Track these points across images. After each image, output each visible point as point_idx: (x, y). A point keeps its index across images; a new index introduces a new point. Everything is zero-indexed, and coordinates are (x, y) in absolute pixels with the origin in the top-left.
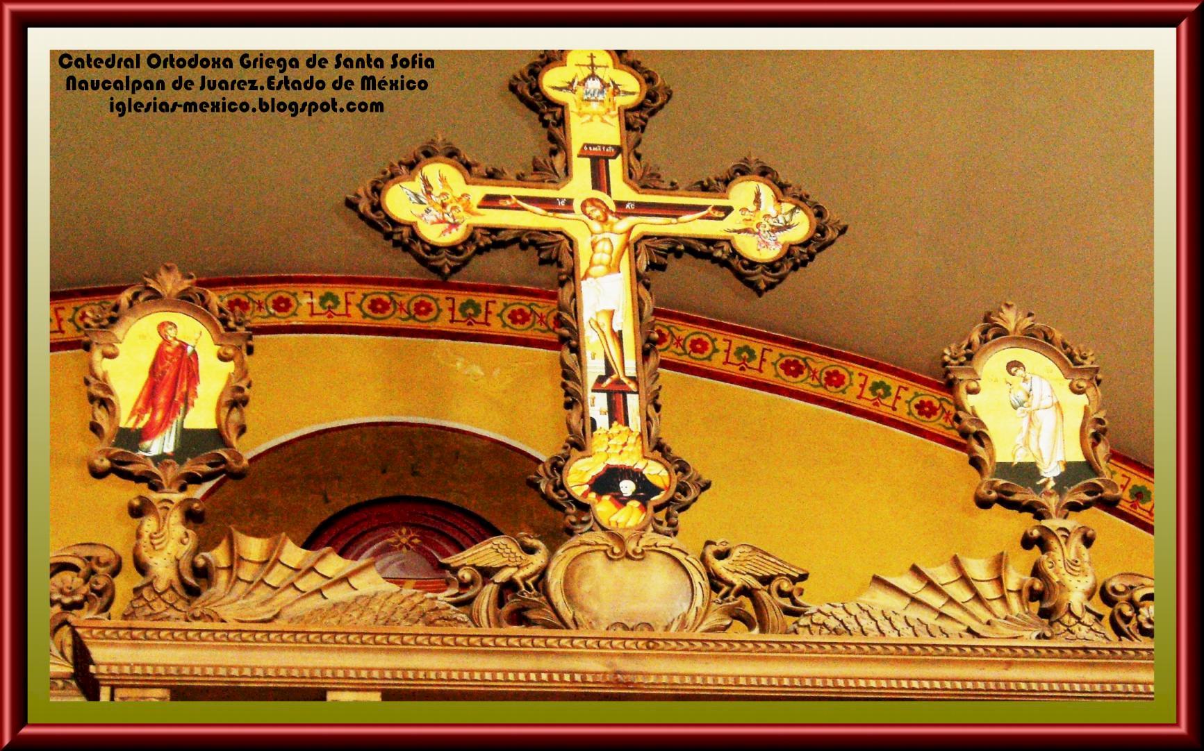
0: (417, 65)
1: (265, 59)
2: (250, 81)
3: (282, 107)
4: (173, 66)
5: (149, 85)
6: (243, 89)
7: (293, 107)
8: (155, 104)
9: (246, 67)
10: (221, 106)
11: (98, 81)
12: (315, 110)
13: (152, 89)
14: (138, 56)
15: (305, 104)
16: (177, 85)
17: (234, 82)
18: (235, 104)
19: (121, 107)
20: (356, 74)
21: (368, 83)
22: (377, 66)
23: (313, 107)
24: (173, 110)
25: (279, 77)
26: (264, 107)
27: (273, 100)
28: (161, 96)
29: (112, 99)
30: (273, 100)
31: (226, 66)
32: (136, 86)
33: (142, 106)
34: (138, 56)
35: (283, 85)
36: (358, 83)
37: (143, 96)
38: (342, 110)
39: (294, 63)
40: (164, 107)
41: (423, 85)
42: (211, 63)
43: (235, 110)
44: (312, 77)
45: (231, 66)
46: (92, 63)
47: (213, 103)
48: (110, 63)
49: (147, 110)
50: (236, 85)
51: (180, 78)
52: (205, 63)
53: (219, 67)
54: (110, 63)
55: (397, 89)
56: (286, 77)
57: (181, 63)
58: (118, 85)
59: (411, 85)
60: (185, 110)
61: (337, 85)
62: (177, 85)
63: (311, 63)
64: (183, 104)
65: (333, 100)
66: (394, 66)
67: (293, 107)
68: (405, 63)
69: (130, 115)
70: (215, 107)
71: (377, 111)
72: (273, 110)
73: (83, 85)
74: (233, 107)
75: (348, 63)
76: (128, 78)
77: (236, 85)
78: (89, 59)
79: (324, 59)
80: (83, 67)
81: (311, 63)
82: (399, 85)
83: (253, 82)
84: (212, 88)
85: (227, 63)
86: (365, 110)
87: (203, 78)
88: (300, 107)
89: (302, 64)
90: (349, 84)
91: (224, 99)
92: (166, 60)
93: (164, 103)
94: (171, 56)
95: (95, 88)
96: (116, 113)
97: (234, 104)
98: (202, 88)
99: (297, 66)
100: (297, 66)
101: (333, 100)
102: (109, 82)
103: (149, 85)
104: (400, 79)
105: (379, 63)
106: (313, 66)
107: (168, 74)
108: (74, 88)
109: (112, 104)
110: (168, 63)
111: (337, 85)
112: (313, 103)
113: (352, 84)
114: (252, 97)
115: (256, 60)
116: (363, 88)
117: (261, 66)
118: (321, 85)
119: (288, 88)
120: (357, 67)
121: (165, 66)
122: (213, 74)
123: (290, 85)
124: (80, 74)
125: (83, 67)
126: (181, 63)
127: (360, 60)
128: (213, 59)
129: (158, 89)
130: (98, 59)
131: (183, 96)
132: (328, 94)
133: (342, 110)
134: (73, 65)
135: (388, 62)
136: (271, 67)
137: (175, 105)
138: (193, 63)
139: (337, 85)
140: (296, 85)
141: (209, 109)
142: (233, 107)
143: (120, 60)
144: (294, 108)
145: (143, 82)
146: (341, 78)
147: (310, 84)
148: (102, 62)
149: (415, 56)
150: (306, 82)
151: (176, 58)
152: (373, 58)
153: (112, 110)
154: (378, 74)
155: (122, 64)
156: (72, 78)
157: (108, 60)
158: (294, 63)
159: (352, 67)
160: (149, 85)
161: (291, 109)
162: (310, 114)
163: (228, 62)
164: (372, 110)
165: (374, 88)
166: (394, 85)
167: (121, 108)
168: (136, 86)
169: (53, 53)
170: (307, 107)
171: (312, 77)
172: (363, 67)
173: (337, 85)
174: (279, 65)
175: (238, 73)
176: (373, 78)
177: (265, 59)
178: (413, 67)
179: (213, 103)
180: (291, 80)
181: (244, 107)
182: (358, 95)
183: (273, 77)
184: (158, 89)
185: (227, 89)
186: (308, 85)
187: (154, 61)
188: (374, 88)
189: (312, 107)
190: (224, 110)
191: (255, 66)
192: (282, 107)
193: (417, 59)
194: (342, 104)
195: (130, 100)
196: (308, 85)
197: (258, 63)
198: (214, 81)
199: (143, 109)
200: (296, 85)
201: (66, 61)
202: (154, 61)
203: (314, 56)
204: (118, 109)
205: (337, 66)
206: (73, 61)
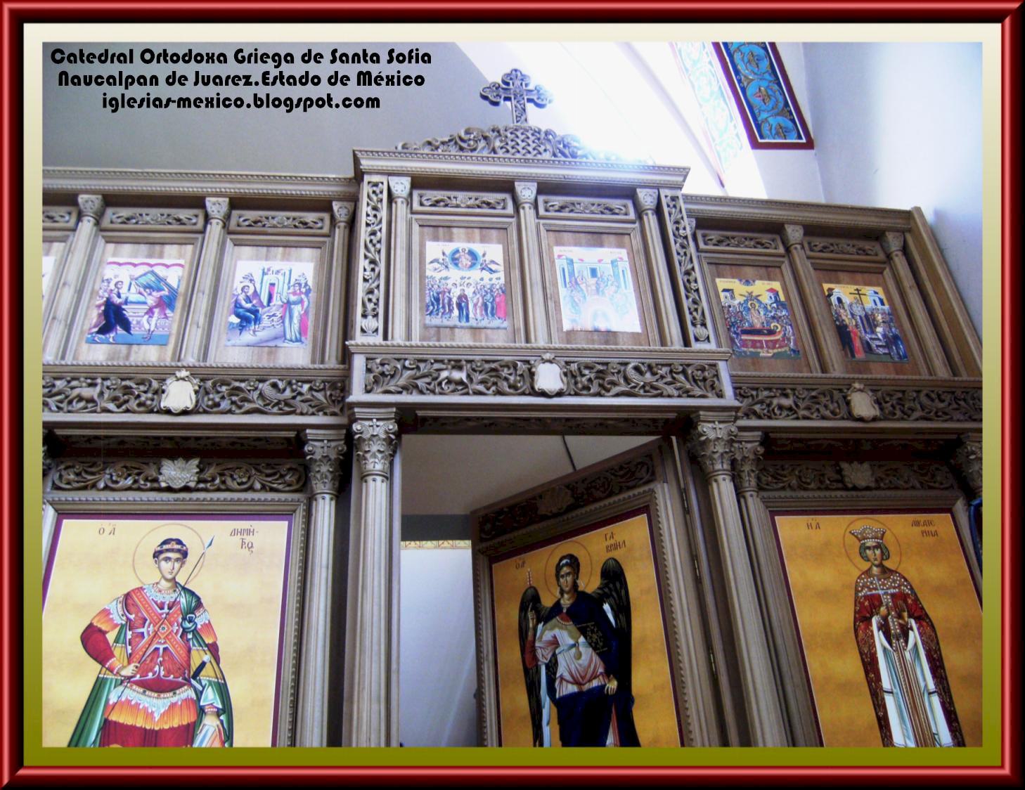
0: (413, 61)
2: (244, 77)
3: (277, 103)
4: (166, 61)
5: (142, 80)
6: (238, 84)
7: (288, 102)
8: (148, 99)
9: (241, 62)
10: (215, 102)
11: (91, 77)
12: (310, 106)
13: (145, 84)
14: (131, 51)
15: (300, 100)
16: (171, 80)
17: (228, 77)
18: (229, 100)
19: (114, 102)
20: (351, 70)
21: (364, 78)
22: (373, 61)
23: (308, 103)
24: (167, 106)
25: (274, 72)
26: (258, 103)
27: (268, 95)
28: (154, 92)
29: (105, 94)
30: (268, 95)
31: (220, 62)
32: (130, 81)
33: (135, 102)
34: (131, 51)
35: (278, 81)
36: (354, 79)
37: (137, 92)
38: (337, 106)
39: (289, 58)
40: (157, 103)
41: (420, 80)
42: (205, 58)
43: (229, 106)
44: (307, 73)
45: (225, 61)
46: (85, 58)
47: (207, 99)
48: (103, 58)
49: (140, 106)
50: (230, 81)
51: (174, 73)
52: (199, 58)
53: (213, 62)
54: (103, 58)
55: (393, 84)
56: (281, 73)
57: (175, 58)
58: (111, 81)
60: (179, 106)
61: (333, 80)
62: (171, 80)
63: (306, 58)
64: (176, 99)
65: (329, 95)
66: (390, 61)
67: (288, 102)
68: (401, 58)
69: (124, 111)
70: (209, 103)
71: (373, 106)
72: (268, 106)
73: (76, 81)
74: (227, 103)
75: (344, 58)
76: (121, 73)
77: (230, 81)
78: (82, 55)
79: (319, 54)
80: (75, 62)
82: (395, 80)
83: (247, 77)
84: (206, 84)
85: (222, 58)
86: (360, 106)
87: (197, 73)
88: (295, 102)
89: (298, 58)
90: (345, 80)
91: (218, 94)
92: (159, 55)
93: (157, 99)
94: (165, 51)
95: (88, 84)
96: (109, 108)
97: (229, 99)
98: (196, 84)
99: (292, 62)
100: (292, 61)
101: (329, 95)
103: (142, 81)
104: (396, 75)
105: (375, 58)
106: (308, 62)
108: (67, 84)
109: (105, 99)
110: (162, 58)
111: (333, 81)
112: (308, 99)
113: (348, 79)
114: (247, 93)
115: (250, 55)
116: (359, 84)
117: (256, 62)
118: (316, 81)
119: (283, 84)
120: (353, 62)
121: (158, 61)
122: (207, 69)
123: (285, 81)
125: (75, 62)
126: (175, 58)
127: (356, 55)
128: (208, 54)
129: (151, 84)
130: (91, 54)
131: (177, 92)
132: (322, 90)
133: (337, 106)
134: (66, 59)
135: (384, 57)
136: (266, 62)
137: (169, 100)
138: (187, 58)
139: (333, 81)
140: (291, 81)
141: (203, 105)
142: (227, 103)
143: (113, 55)
144: (289, 104)
146: (336, 73)
147: (305, 80)
148: (94, 57)
149: (411, 51)
150: (302, 77)
151: (170, 53)
152: (369, 53)
153: (105, 106)
154: (374, 69)
155: (115, 59)
156: (64, 73)
157: (101, 55)
158: (289, 58)
159: (348, 62)
160: (142, 81)
161: (287, 106)
162: (305, 110)
163: (222, 58)
164: (368, 106)
165: (370, 84)
166: (390, 80)
167: (114, 104)
168: (130, 81)
169: (45, 45)
170: (302, 104)
171: (307, 73)
172: (359, 62)
173: (333, 80)
174: (274, 61)
175: (232, 68)
176: (369, 73)
178: (410, 62)
179: (207, 99)
180: (286, 75)
181: (239, 103)
182: (354, 90)
183: (267, 73)
184: (151, 84)
185: (221, 84)
186: (304, 81)
187: (148, 56)
188: (370, 84)
189: (308, 103)
190: (218, 106)
191: (249, 62)
192: (277, 103)
193: (414, 54)
195: (123, 95)
196: (304, 81)
197: (253, 59)
198: (209, 77)
199: (136, 105)
200: (291, 81)
201: (58, 56)
202: (148, 56)
203: (310, 51)
204: (111, 105)
205: (333, 61)
206: (66, 56)
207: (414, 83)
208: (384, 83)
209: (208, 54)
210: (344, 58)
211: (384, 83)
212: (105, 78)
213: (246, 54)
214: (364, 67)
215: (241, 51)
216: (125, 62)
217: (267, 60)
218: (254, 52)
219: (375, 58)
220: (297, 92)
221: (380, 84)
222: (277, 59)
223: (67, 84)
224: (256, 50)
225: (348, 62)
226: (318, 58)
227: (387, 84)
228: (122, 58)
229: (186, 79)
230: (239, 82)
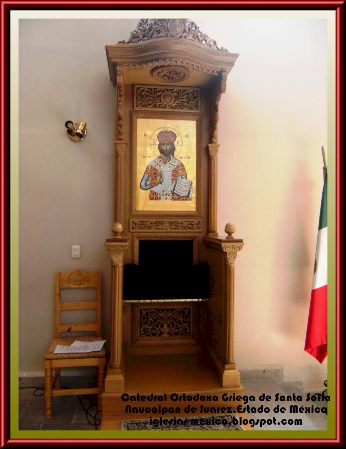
0: (321, 400)
1: (236, 396)
2: (228, 408)
4: (185, 400)
7: (252, 422)
9: (226, 400)
12: (264, 424)
15: (258, 420)
17: (219, 409)
20: (287, 405)
21: (293, 409)
22: (298, 400)
23: (263, 422)
24: (185, 424)
25: (244, 406)
27: (241, 418)
32: (164, 411)
35: (246, 410)
36: (288, 409)
39: (252, 398)
42: (206, 398)
44: (262, 406)
51: (189, 406)
53: (210, 400)
54: (150, 398)
56: (248, 406)
59: (318, 410)
60: (192, 424)
61: (276, 410)
63: (262, 398)
65: (274, 418)
66: (308, 400)
67: (252, 422)
71: (298, 424)
76: (160, 406)
77: (220, 410)
81: (262, 398)
82: (311, 410)
84: (206, 412)
86: (291, 424)
88: (256, 422)
89: (257, 399)
92: (181, 397)
101: (274, 418)
102: (150, 409)
104: (311, 407)
107: (183, 404)
110: (182, 399)
112: (262, 420)
113: (285, 409)
115: (231, 397)
116: (291, 412)
117: (234, 400)
119: (249, 412)
120: (288, 400)
121: (180, 400)
122: (207, 404)
123: (250, 410)
124: (133, 405)
125: (135, 400)
127: (289, 397)
128: (207, 396)
129: (176, 412)
133: (279, 424)
134: (129, 399)
135: (305, 398)
136: (239, 401)
140: (253, 410)
145: (168, 408)
146: (278, 406)
147: (261, 410)
150: (259, 409)
152: (296, 395)
154: (299, 404)
155: (157, 399)
158: (252, 398)
159: (284, 400)
161: (251, 423)
164: (295, 424)
166: (308, 410)
170: (259, 422)
172: (291, 400)
174: (244, 400)
176: (296, 406)
177: (236, 396)
178: (319, 400)
182: (288, 415)
183: (241, 406)
184: (176, 412)
186: (260, 410)
188: (297, 412)
191: (230, 400)
194: (279, 420)
196: (260, 410)
197: (232, 399)
200: (253, 410)
201: (125, 397)
203: (264, 395)
205: (276, 400)
207: (321, 411)
208: (304, 411)
209: (207, 396)
210: (283, 398)
211: (304, 411)
212: (151, 409)
213: (228, 396)
214: (293, 403)
215: (226, 394)
216: (162, 400)
217: (240, 399)
218: (233, 395)
219: (300, 398)
220: (257, 416)
221: (302, 412)
222: (246, 399)
223: (130, 412)
224: (234, 394)
225: (284, 400)
226: (268, 398)
227: (306, 412)
228: (160, 398)
229: (196, 409)
230: (225, 411)
